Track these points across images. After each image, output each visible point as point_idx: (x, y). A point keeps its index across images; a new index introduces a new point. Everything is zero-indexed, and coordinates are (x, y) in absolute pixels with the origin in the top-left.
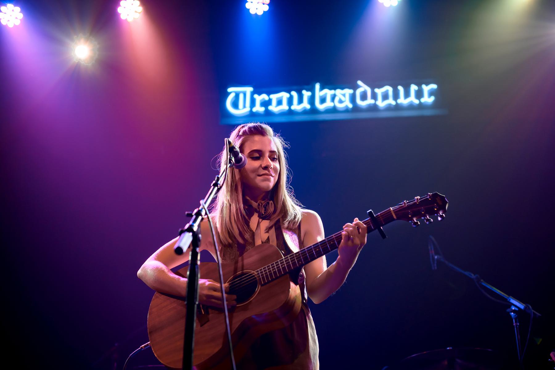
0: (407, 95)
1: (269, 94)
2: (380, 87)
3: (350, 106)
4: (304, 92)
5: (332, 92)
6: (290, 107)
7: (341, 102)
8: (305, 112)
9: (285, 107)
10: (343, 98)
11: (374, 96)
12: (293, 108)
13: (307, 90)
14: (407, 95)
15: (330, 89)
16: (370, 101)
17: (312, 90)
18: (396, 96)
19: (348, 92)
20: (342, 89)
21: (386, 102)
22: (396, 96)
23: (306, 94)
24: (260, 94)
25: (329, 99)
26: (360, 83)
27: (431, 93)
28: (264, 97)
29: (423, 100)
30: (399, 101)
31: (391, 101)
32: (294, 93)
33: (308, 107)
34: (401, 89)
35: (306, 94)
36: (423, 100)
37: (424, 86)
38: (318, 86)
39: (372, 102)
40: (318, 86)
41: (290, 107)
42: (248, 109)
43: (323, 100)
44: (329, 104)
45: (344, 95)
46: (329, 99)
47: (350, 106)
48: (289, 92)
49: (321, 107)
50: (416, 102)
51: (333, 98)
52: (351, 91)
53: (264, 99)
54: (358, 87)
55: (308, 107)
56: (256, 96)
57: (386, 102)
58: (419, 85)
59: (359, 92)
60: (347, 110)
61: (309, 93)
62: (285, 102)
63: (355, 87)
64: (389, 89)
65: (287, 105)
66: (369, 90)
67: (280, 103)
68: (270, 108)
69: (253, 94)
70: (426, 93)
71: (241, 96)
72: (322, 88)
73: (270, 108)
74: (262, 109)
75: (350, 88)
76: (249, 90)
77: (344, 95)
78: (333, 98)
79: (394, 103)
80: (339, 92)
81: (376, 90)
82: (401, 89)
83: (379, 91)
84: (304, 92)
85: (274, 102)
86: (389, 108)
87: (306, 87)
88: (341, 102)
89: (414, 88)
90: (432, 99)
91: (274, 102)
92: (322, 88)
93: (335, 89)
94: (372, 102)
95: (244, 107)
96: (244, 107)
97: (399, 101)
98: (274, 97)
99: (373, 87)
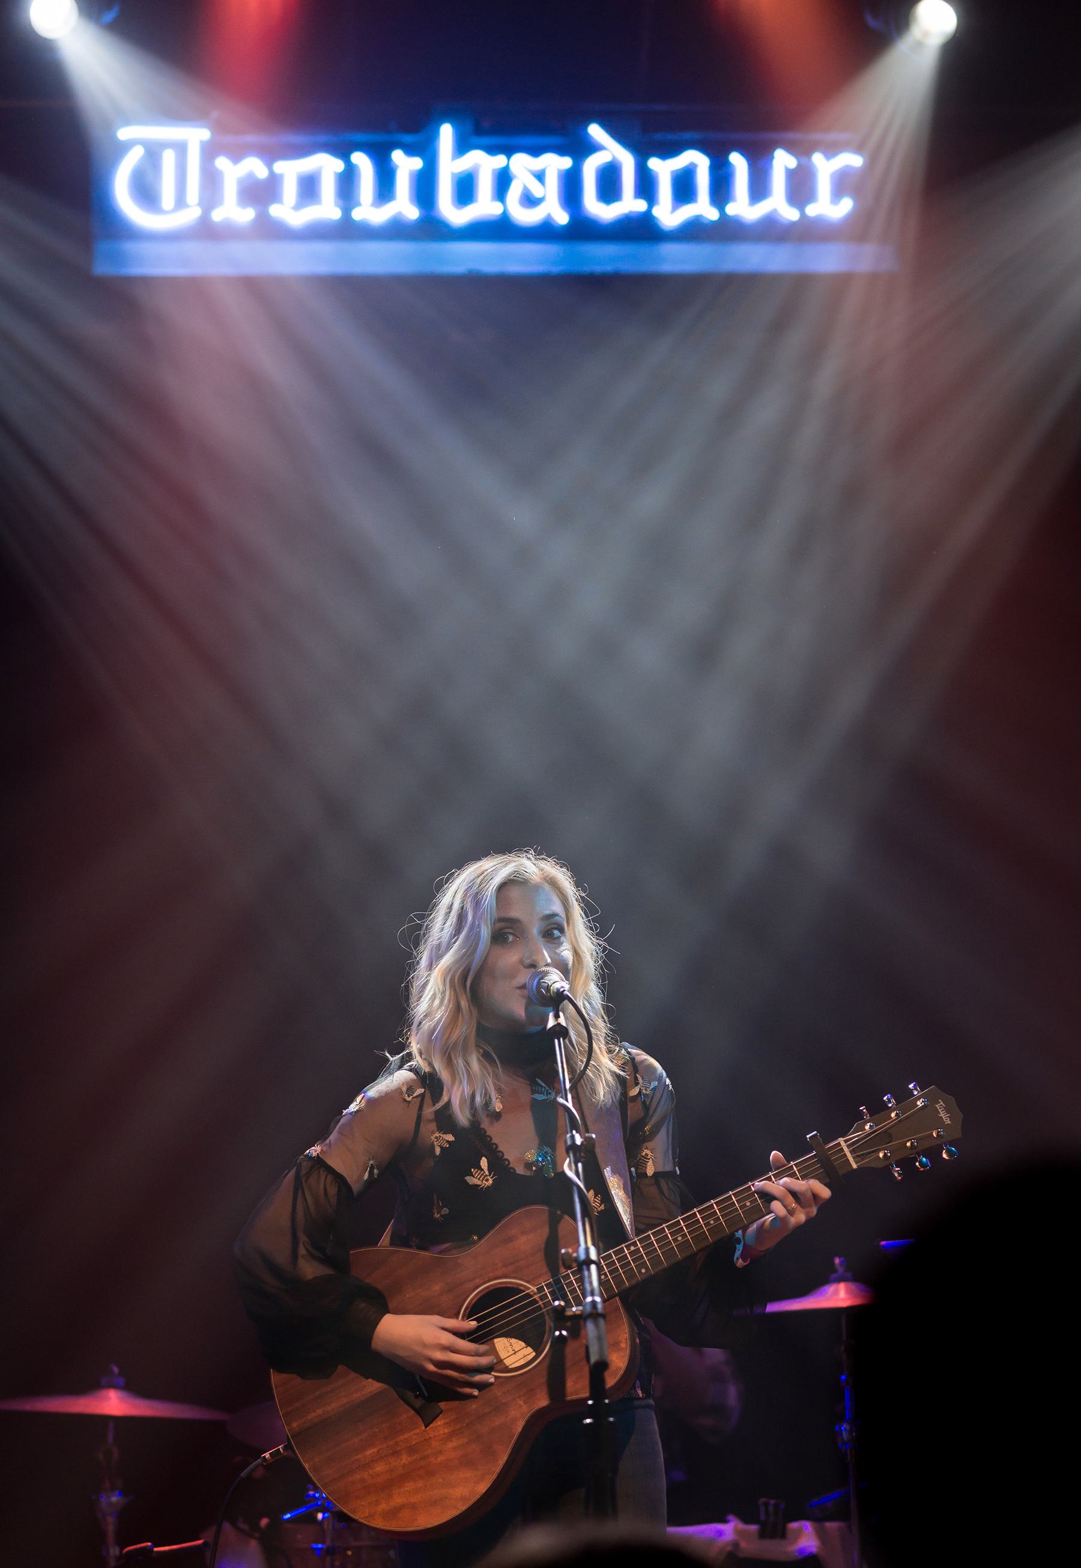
0: (759, 189)
1: (270, 156)
2: (668, 151)
3: (562, 218)
4: (398, 156)
5: (499, 161)
6: (347, 211)
7: (529, 201)
8: (396, 230)
9: (328, 209)
10: (537, 190)
11: (646, 187)
12: (357, 215)
13: (411, 150)
14: (759, 189)
15: (492, 150)
16: (630, 204)
17: (426, 149)
18: (721, 190)
19: (555, 163)
20: (536, 151)
21: (687, 212)
22: (721, 190)
23: (406, 165)
24: (236, 157)
25: (485, 186)
26: (596, 131)
27: (842, 184)
28: (255, 167)
29: (812, 210)
30: (731, 209)
31: (703, 208)
32: (361, 160)
33: (412, 213)
34: (738, 161)
35: (406, 165)
36: (812, 210)
37: (817, 158)
38: (446, 133)
39: (641, 206)
40: (446, 133)
41: (347, 211)
42: (191, 215)
43: (465, 190)
44: (485, 207)
45: (540, 177)
46: (485, 186)
47: (562, 218)
48: (343, 152)
49: (455, 216)
50: (791, 214)
51: (503, 181)
52: (566, 162)
53: (251, 176)
54: (593, 147)
55: (412, 213)
56: (222, 163)
57: (687, 212)
58: (802, 150)
59: (591, 166)
60: (545, 232)
61: (416, 163)
62: (328, 188)
63: (581, 149)
64: (697, 160)
65: (336, 205)
66: (627, 161)
67: (309, 187)
68: (276, 211)
69: (209, 152)
70: (824, 186)
71: (169, 158)
72: (462, 147)
73: (276, 211)
74: (246, 216)
75: (561, 151)
76: (196, 136)
77: (540, 177)
78: (503, 181)
79: (712, 214)
80: (521, 164)
81: (654, 163)
82: (738, 161)
83: (663, 169)
84: (398, 156)
85: (290, 190)
86: (693, 231)
87: (408, 138)
88: (529, 201)
89: (782, 160)
90: (846, 206)
91: (290, 190)
92: (462, 147)
93: (509, 151)
94: (641, 206)
95: (181, 202)
96: (181, 202)
97: (731, 209)
98: (290, 170)
99: (642, 151)
